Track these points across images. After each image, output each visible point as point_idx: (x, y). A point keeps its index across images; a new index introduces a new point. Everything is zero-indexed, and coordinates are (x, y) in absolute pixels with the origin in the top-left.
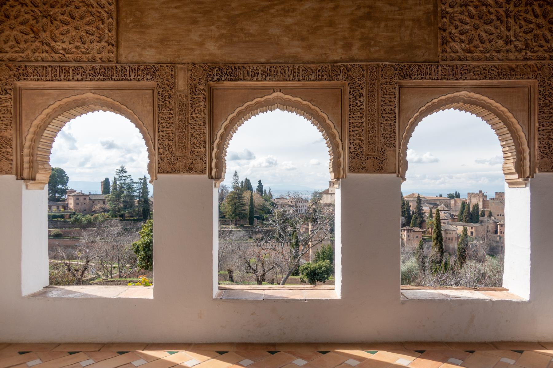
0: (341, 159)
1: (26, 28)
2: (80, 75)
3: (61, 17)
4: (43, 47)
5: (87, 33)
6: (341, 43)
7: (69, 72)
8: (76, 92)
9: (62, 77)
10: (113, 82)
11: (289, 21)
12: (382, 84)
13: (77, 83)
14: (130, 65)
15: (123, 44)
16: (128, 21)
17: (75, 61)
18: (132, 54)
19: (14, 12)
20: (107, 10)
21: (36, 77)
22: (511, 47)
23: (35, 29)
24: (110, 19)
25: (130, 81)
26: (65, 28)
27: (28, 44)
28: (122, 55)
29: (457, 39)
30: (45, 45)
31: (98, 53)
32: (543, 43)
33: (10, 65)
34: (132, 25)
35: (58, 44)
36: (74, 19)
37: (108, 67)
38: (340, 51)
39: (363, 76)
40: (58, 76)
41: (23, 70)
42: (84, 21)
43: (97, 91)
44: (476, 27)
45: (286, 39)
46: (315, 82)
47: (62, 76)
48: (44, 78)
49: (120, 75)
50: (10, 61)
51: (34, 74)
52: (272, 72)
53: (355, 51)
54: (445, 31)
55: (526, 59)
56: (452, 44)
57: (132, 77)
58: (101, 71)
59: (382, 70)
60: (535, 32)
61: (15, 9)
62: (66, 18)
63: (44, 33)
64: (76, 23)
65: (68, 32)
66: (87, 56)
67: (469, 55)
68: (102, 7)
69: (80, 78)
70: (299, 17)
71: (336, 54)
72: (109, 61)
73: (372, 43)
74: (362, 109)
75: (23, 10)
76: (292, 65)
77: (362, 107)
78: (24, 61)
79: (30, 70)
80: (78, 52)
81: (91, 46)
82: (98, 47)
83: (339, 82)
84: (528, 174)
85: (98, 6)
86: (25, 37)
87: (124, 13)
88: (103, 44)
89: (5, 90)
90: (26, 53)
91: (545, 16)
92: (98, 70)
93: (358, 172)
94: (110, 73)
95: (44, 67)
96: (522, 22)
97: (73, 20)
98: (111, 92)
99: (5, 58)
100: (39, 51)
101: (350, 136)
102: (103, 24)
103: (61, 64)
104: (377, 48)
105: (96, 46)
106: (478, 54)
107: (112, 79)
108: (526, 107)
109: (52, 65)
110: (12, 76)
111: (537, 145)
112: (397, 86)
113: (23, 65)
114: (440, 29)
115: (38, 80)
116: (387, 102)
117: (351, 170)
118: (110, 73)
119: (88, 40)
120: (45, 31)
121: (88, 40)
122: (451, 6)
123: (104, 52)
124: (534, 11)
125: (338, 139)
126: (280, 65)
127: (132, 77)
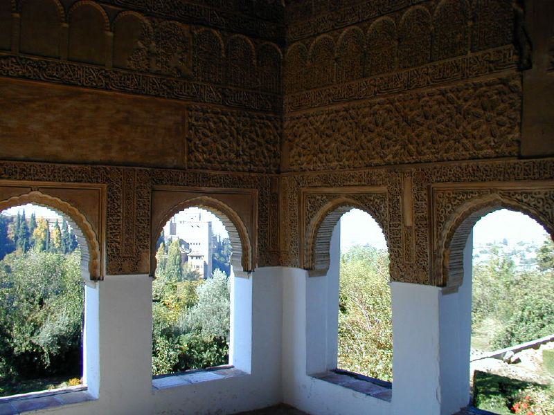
0: (98, 260)
6: (101, 145)
11: (50, 118)
12: (137, 188)
22: (240, 160)
29: (200, 150)
32: (263, 159)
38: (99, 153)
39: (121, 180)
44: (215, 141)
45: (47, 136)
46: (76, 183)
52: (32, 172)
53: (114, 155)
54: (191, 141)
55: (250, 171)
56: (197, 154)
59: (138, 175)
60: (256, 149)
67: (209, 164)
70: (60, 115)
71: (98, 156)
73: (129, 147)
74: (119, 212)
76: (53, 164)
77: (118, 210)
83: (99, 184)
84: (250, 269)
91: (263, 136)
93: (115, 274)
96: (248, 140)
101: (107, 238)
104: (134, 153)
106: (216, 165)
108: (249, 212)
111: (257, 244)
112: (150, 191)
114: (187, 138)
116: (141, 205)
117: (108, 273)
122: (196, 120)
124: (256, 131)
125: (94, 240)
126: (40, 164)
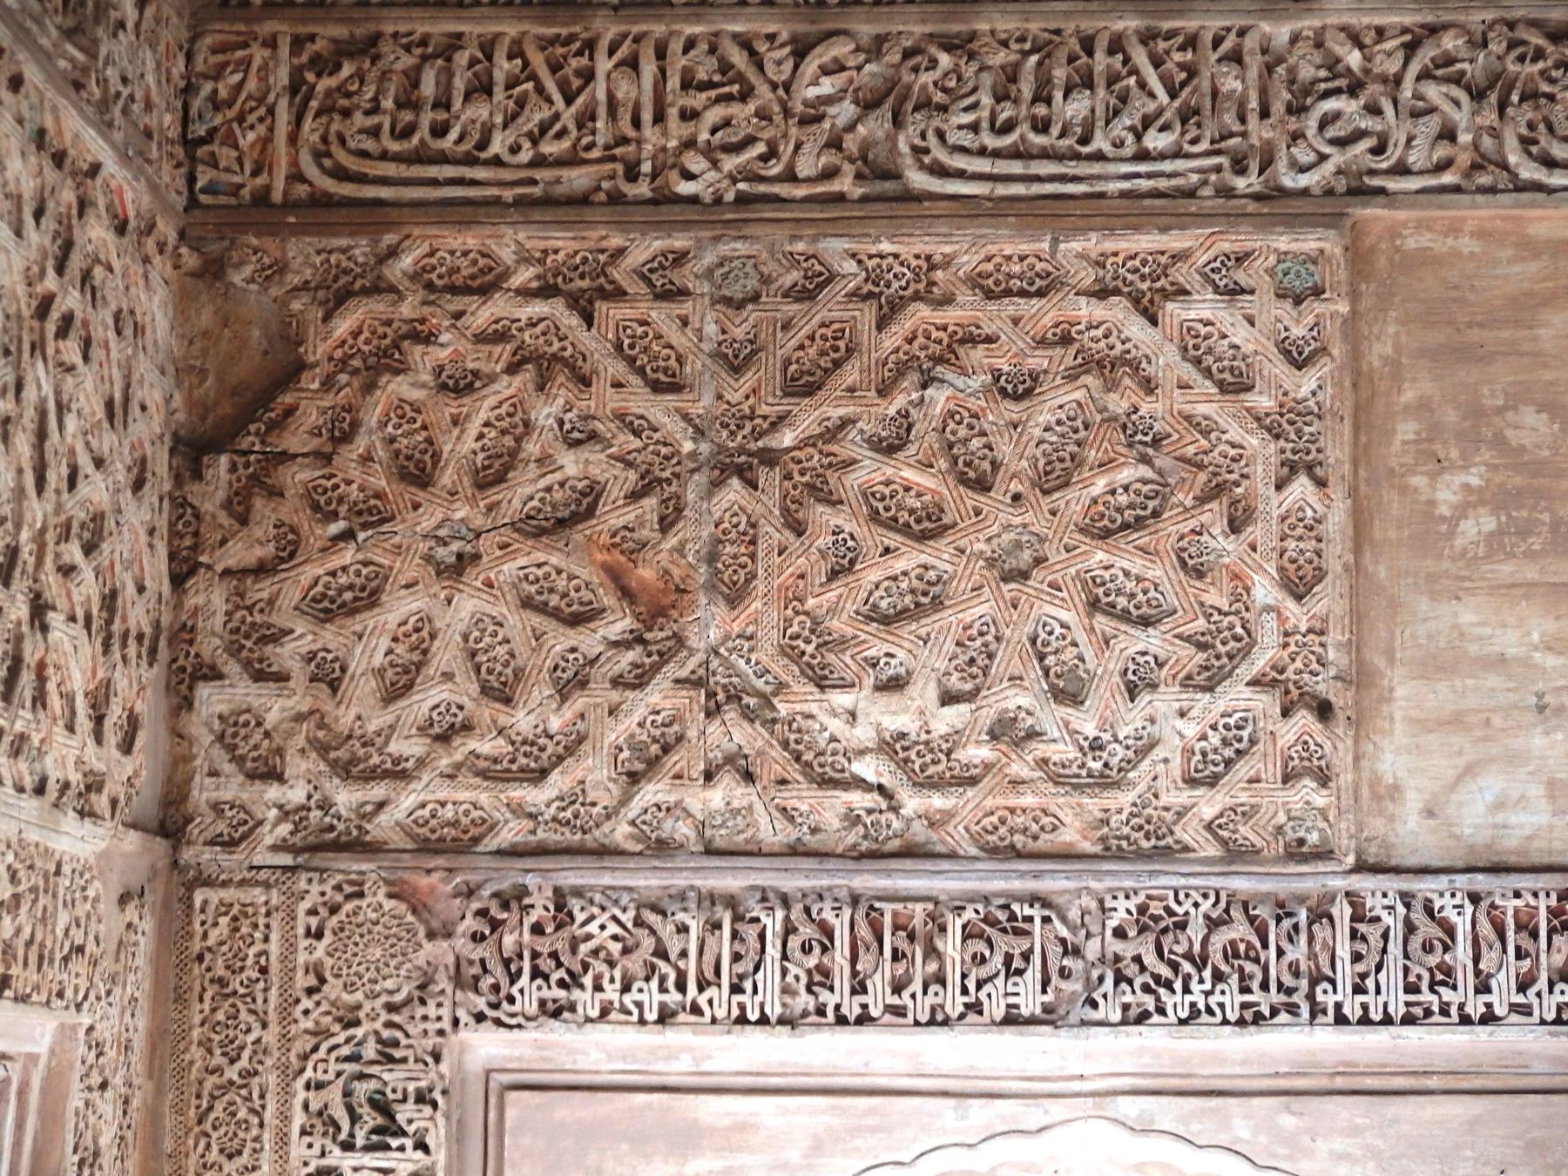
1: (571, 566)
2: (1033, 974)
3: (870, 471)
4: (714, 728)
5: (1094, 605)
7: (931, 952)
8: (982, 1114)
9: (878, 996)
10: (1325, 1041)
13: (1010, 1038)
14: (1481, 882)
15: (1405, 694)
16: (1447, 495)
17: (993, 852)
18: (1491, 785)
19: (474, 428)
20: (1263, 401)
21: (651, 997)
23: (646, 573)
24: (1302, 487)
25: (1483, 1032)
26: (909, 559)
27: (579, 702)
28: (1395, 791)
30: (731, 714)
31: (1192, 782)
33: (424, 881)
34: (1483, 523)
35: (842, 699)
36: (982, 485)
37: (1283, 910)
40: (843, 981)
41: (537, 929)
42: (1074, 501)
43: (1166, 1111)
47: (879, 985)
48: (719, 1000)
49: (1392, 977)
50: (427, 847)
51: (635, 964)
57: (1502, 995)
58: (1220, 939)
61: (483, 409)
62: (915, 477)
63: (721, 610)
64: (998, 522)
65: (928, 599)
66: (1093, 804)
68: (1235, 385)
69: (1030, 1000)
72: (1298, 853)
75: (545, 413)
78: (542, 851)
79: (601, 931)
80: (1018, 769)
81: (1131, 719)
82: (1191, 730)
85: (1188, 371)
86: (561, 640)
87: (1407, 430)
88: (1236, 696)
89: (381, 1105)
90: (558, 782)
92: (1196, 931)
94: (1297, 952)
95: (711, 899)
97: (972, 499)
98: (1288, 1121)
99: (383, 826)
100: (676, 761)
102: (1235, 527)
103: (868, 881)
105: (1180, 722)
107: (1316, 1010)
109: (791, 883)
110: (443, 983)
113: (539, 885)
115: (665, 1017)
118: (1297, 952)
119: (1106, 669)
120: (735, 597)
121: (1106, 669)
123: (1243, 769)
127: (1502, 995)
